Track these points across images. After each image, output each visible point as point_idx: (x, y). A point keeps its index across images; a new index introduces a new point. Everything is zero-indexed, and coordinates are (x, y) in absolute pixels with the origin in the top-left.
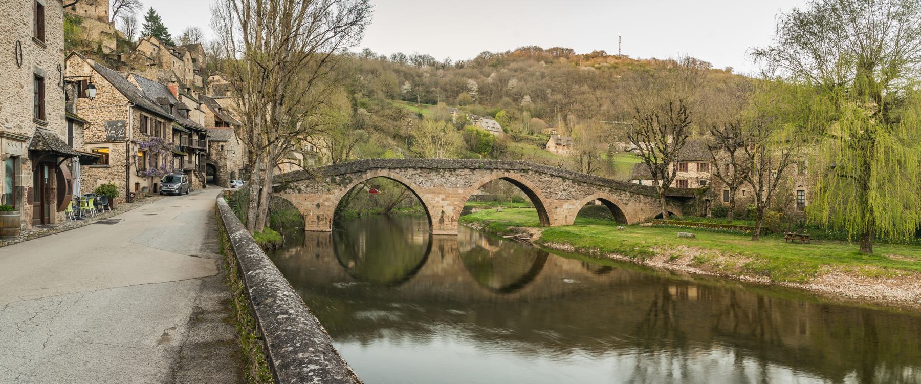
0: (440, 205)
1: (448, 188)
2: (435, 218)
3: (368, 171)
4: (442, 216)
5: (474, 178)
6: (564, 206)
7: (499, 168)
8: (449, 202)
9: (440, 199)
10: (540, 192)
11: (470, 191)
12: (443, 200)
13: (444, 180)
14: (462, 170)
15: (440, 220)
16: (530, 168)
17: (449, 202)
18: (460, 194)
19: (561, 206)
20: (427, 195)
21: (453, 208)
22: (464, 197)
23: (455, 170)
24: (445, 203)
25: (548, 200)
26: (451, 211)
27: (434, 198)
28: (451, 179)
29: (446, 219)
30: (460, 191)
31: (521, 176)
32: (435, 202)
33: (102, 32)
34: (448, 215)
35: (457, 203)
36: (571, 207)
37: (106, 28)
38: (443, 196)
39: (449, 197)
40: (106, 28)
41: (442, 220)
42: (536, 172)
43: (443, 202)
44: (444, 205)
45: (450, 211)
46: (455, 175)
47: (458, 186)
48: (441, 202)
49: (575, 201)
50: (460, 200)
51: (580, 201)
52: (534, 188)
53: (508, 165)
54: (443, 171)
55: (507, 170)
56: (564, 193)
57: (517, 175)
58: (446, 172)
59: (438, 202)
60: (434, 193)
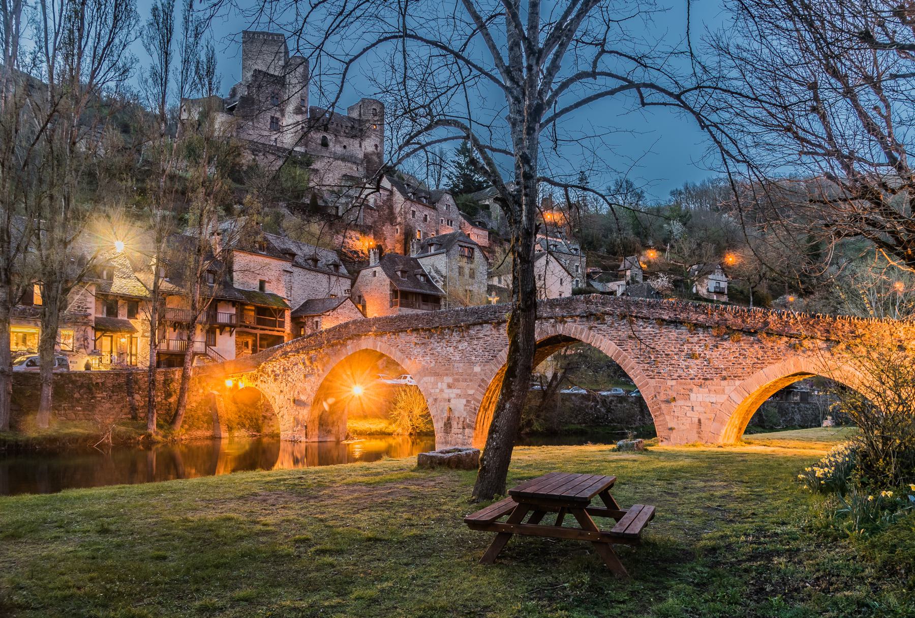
0: (446, 396)
1: (456, 365)
2: (437, 421)
3: (349, 342)
4: (449, 418)
5: (499, 341)
6: (693, 396)
7: (545, 315)
8: (459, 391)
9: (445, 386)
10: (633, 362)
11: (493, 367)
12: (449, 386)
13: (451, 350)
14: (479, 327)
15: (445, 425)
16: (608, 309)
17: (459, 391)
18: (476, 374)
19: (687, 397)
20: (425, 379)
21: (464, 401)
22: (483, 380)
23: (468, 327)
24: (451, 393)
25: (653, 382)
26: (462, 407)
27: (437, 384)
28: (464, 345)
29: (454, 424)
30: (477, 369)
31: (590, 328)
32: (438, 391)
33: (344, 176)
34: (457, 414)
35: (471, 392)
36: (713, 398)
37: (351, 169)
38: (449, 380)
39: (457, 380)
40: (351, 169)
41: (448, 425)
42: (623, 317)
43: (450, 391)
44: (452, 396)
45: (459, 406)
46: (468, 339)
47: (474, 358)
48: (447, 391)
49: (724, 383)
50: (476, 386)
51: (737, 383)
52: (619, 354)
53: (562, 308)
54: (450, 332)
55: (562, 320)
56: (692, 362)
57: (580, 327)
58: (454, 334)
59: (442, 391)
60: (436, 374)
